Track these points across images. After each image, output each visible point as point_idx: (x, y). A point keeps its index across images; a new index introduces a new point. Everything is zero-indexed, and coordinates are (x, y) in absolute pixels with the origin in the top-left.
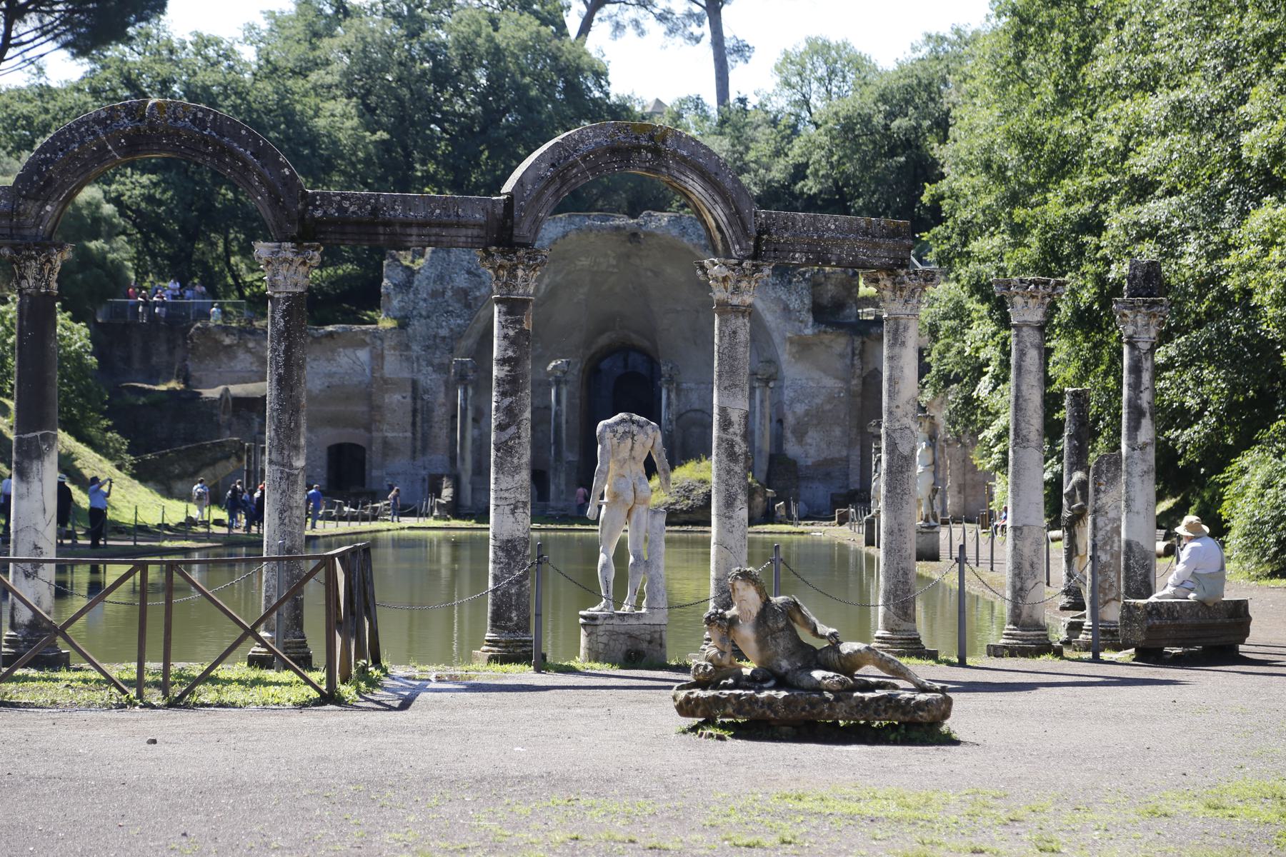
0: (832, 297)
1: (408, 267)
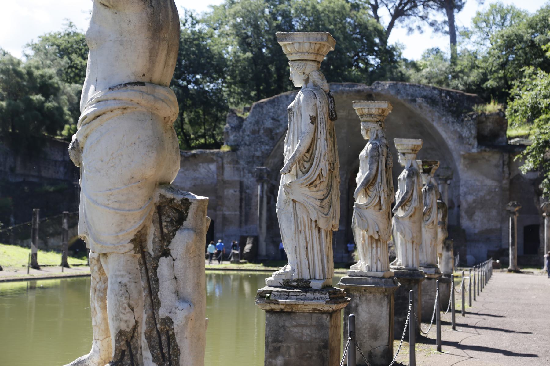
0: (490, 130)
1: (240, 118)
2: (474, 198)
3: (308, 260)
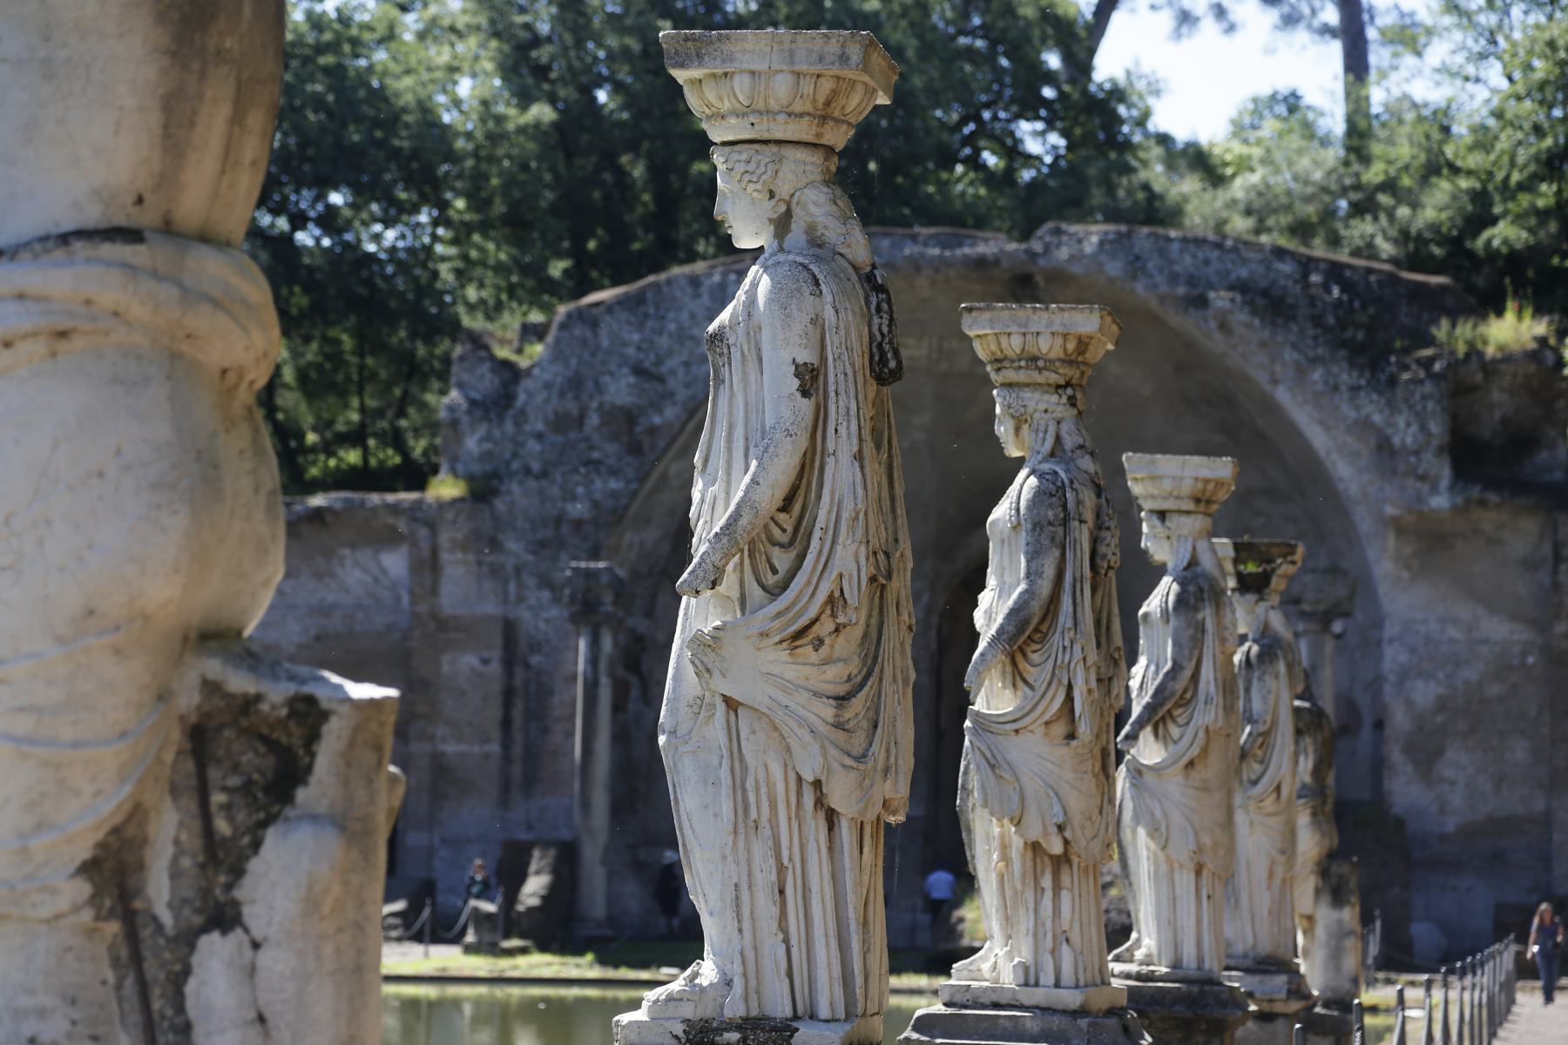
0: (1504, 421)
1: (506, 365)
2: (1441, 690)
3: (786, 941)
